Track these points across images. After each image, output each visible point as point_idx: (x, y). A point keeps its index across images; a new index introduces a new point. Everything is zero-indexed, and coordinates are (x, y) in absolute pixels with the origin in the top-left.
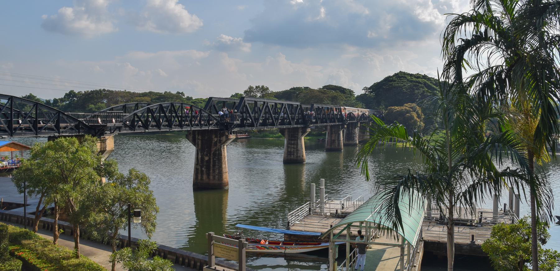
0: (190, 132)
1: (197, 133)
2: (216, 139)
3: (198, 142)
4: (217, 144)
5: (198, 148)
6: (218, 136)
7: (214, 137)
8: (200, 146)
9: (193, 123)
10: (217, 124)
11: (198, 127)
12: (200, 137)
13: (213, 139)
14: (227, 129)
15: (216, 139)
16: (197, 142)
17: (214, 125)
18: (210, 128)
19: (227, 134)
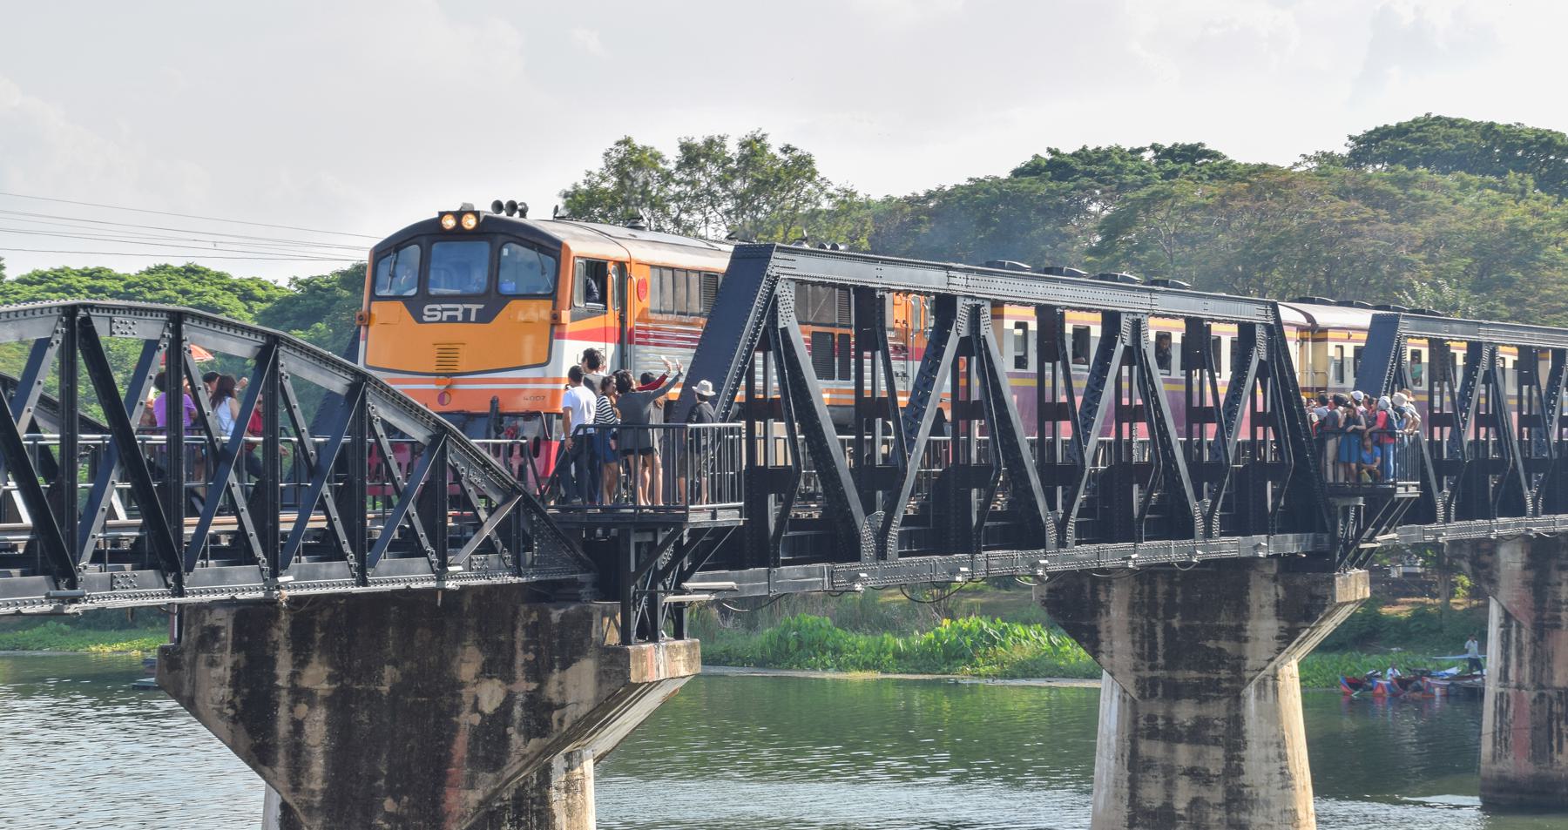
0: (209, 620)
1: (280, 632)
2: (490, 695)
3: (298, 726)
4: (505, 738)
5: (296, 788)
6: (520, 659)
7: (468, 665)
8: (318, 766)
9: (287, 521)
10: (512, 538)
11: (336, 566)
12: (317, 676)
13: (466, 694)
14: (611, 586)
15: (490, 695)
16: (283, 727)
17: (487, 547)
18: (462, 573)
19: (613, 638)
